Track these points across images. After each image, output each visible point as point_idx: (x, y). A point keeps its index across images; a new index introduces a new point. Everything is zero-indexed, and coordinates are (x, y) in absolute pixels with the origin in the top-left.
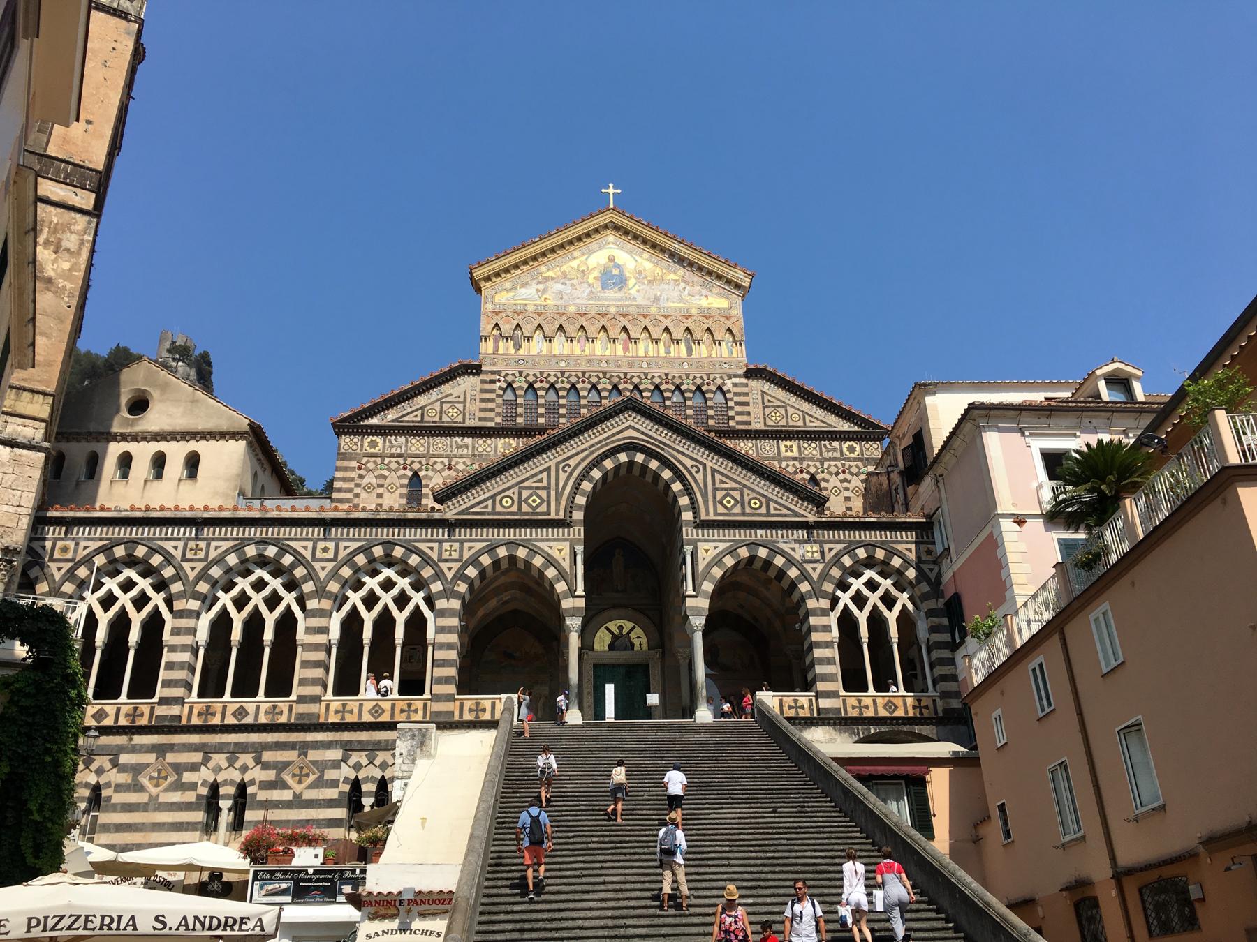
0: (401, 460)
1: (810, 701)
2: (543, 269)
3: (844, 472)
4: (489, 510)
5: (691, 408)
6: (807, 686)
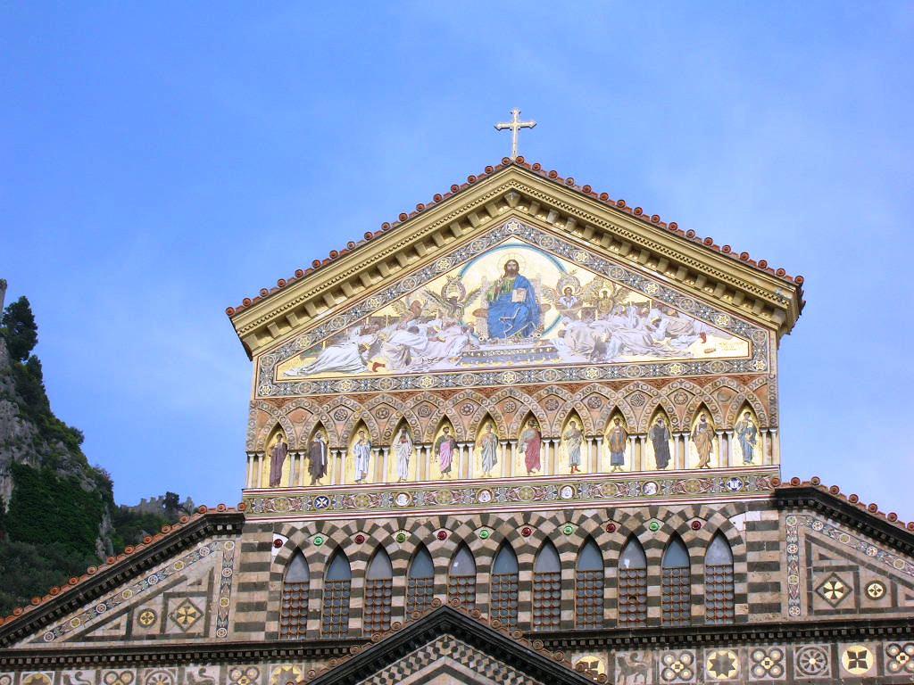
2: (374, 301)
5: (656, 580)
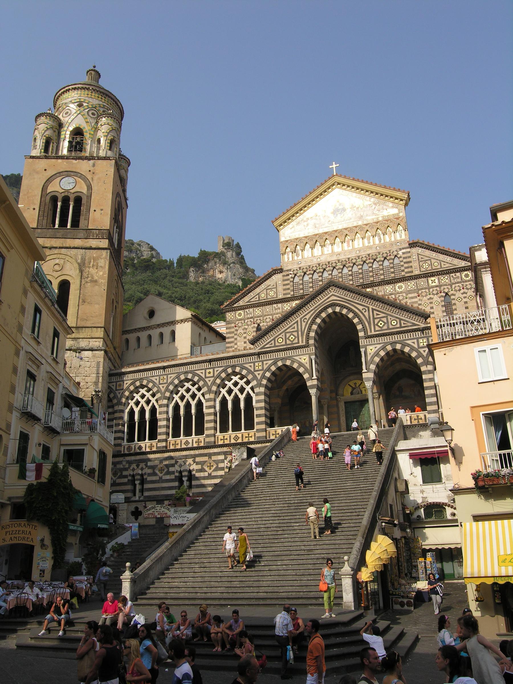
0: (252, 320)
1: (425, 416)
3: (463, 288)
4: (273, 345)
6: (424, 409)
